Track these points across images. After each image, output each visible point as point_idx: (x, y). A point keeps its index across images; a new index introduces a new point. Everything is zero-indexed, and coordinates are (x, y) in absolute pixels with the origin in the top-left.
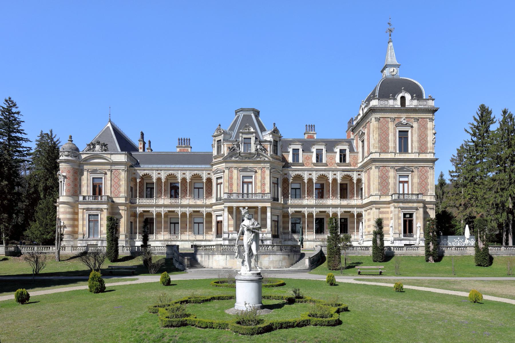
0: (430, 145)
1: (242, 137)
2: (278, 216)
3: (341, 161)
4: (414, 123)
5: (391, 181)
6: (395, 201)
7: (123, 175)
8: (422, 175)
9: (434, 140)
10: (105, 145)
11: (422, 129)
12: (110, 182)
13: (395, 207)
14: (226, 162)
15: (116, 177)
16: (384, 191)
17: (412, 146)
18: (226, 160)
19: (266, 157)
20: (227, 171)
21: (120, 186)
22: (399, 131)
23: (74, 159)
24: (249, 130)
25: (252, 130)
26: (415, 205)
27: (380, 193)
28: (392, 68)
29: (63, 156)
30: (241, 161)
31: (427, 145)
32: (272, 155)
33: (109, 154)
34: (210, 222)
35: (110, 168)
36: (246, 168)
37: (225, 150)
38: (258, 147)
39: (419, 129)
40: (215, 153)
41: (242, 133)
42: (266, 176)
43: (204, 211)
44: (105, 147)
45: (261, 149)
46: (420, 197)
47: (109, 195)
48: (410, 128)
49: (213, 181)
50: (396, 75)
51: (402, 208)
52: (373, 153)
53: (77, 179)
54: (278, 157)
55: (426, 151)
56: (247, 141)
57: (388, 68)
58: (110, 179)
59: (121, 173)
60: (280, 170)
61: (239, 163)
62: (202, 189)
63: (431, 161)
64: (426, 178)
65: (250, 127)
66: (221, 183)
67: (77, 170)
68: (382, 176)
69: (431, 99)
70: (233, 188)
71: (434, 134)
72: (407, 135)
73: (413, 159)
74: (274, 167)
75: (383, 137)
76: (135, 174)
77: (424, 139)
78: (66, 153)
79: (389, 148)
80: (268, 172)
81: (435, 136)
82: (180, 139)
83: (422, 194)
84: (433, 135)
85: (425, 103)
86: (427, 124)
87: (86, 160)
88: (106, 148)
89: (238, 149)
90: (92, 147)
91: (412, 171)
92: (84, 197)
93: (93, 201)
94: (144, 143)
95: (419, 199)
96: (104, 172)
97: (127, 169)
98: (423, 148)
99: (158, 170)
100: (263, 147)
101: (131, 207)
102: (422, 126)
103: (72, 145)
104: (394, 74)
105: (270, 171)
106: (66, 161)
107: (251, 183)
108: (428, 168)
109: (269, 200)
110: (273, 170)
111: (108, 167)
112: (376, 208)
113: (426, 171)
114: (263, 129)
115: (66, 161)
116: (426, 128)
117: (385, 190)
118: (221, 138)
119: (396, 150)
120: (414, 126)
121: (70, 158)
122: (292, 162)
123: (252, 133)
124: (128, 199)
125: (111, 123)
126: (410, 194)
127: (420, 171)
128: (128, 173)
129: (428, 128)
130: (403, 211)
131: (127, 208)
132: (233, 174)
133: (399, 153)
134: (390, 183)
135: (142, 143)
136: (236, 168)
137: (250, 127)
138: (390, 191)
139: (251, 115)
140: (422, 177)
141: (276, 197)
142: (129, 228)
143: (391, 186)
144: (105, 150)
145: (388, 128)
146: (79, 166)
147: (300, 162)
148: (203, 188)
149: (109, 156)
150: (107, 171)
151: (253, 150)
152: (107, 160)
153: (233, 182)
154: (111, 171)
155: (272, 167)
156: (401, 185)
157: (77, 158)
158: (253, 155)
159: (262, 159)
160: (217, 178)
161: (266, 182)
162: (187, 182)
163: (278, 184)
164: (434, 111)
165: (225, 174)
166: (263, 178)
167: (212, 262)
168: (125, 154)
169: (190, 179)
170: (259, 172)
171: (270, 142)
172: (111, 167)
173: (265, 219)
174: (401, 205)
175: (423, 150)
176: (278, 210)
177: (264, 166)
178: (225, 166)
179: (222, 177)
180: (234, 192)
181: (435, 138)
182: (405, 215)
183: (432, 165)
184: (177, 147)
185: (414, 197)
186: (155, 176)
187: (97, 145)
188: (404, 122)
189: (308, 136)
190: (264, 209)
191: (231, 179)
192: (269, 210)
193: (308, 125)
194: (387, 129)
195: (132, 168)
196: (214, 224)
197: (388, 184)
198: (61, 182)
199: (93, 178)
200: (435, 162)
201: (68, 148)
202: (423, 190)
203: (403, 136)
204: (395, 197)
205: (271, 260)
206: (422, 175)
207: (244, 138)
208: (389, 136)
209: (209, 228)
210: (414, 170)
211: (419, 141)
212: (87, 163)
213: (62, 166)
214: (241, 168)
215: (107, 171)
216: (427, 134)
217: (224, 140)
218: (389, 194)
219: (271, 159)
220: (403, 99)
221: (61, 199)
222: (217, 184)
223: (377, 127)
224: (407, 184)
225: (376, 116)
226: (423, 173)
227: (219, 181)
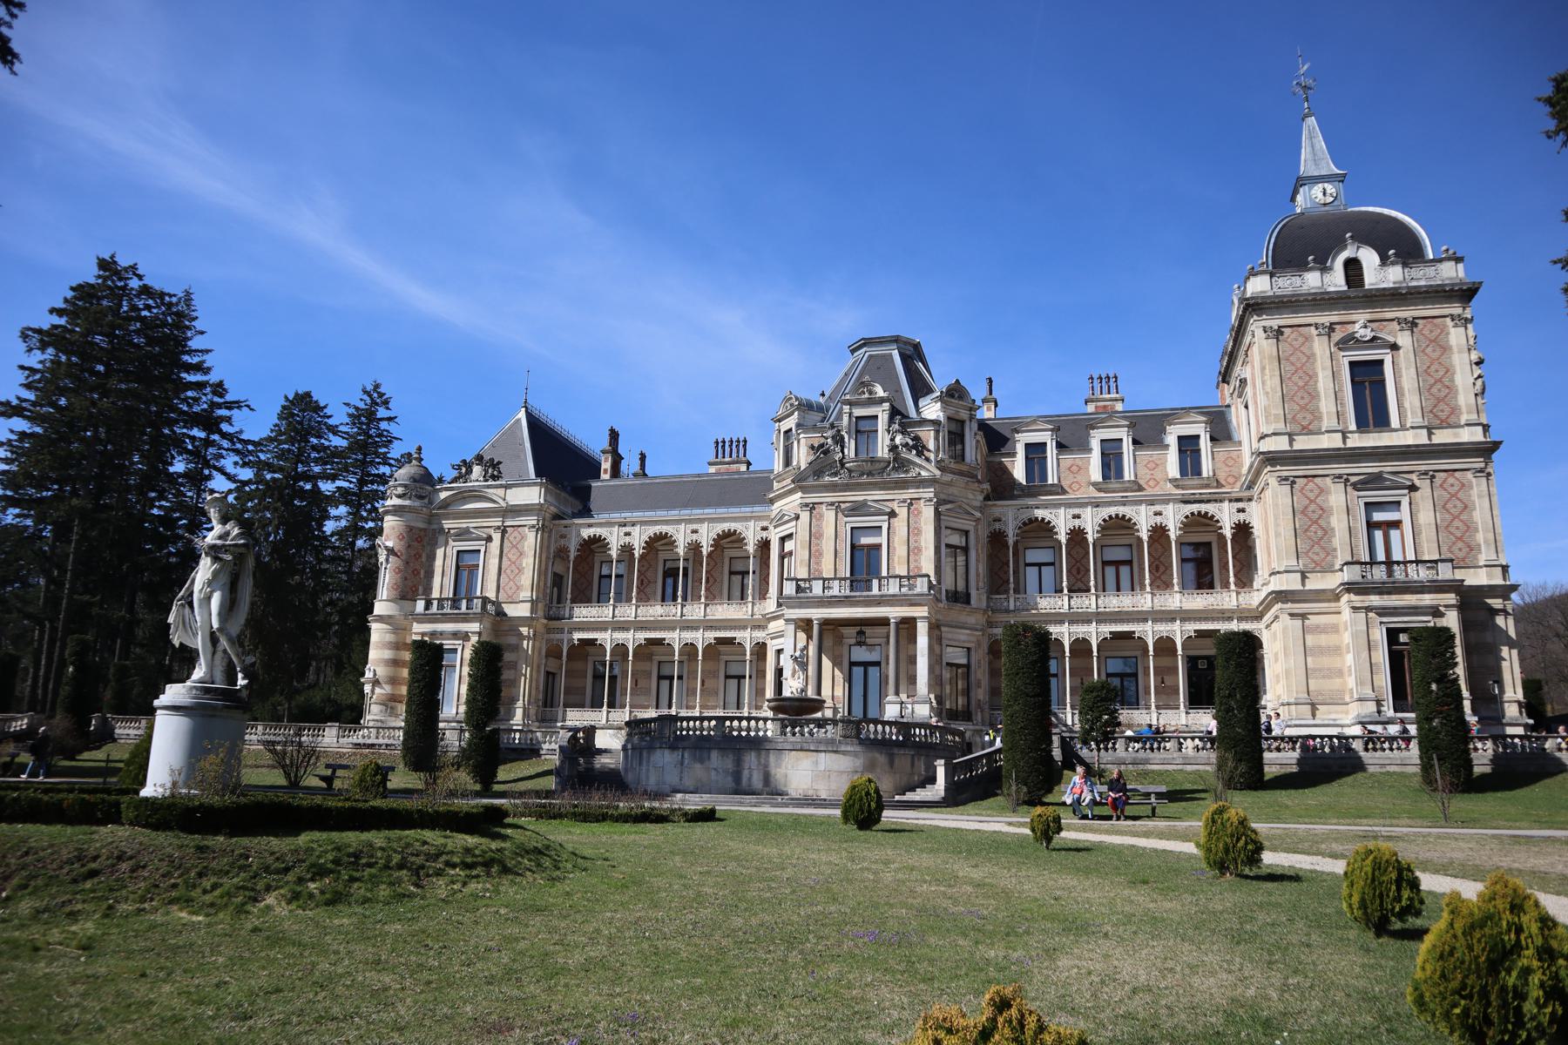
0: (1465, 398)
1: (850, 414)
2: (969, 649)
4: (1399, 333)
5: (1338, 522)
6: (1351, 587)
7: (530, 541)
8: (1449, 500)
9: (1479, 382)
10: (494, 465)
12: (497, 561)
13: (1354, 608)
14: (804, 490)
15: (514, 546)
16: (1316, 558)
17: (1399, 406)
18: (801, 482)
20: (805, 516)
21: (520, 570)
22: (1352, 364)
23: (417, 503)
24: (871, 393)
25: (880, 392)
26: (1427, 599)
27: (1304, 565)
28: (1320, 185)
30: (847, 485)
31: (1456, 400)
32: (942, 460)
33: (501, 486)
35: (500, 524)
36: (864, 504)
37: (802, 457)
38: (899, 439)
40: (778, 466)
41: (851, 404)
42: (922, 524)
43: (746, 637)
44: (494, 468)
46: (1445, 573)
47: (491, 595)
48: (1388, 351)
50: (1335, 203)
51: (1383, 612)
52: (1267, 436)
53: (420, 556)
54: (964, 468)
55: (1452, 420)
56: (864, 426)
57: (1306, 187)
58: (498, 552)
59: (526, 535)
60: (974, 508)
61: (840, 491)
63: (1477, 450)
64: (1466, 507)
65: (873, 386)
66: (790, 553)
67: (422, 533)
68: (1306, 508)
69: (1449, 259)
70: (823, 566)
71: (1477, 364)
72: (1382, 373)
73: (1409, 446)
74: (951, 498)
75: (1296, 384)
76: (563, 536)
78: (400, 490)
79: (1320, 419)
80: (928, 513)
81: (1479, 372)
83: (1451, 561)
84: (1474, 366)
85: (1430, 271)
86: (1448, 334)
87: (446, 504)
88: (495, 473)
89: (838, 449)
90: (464, 470)
91: (1413, 488)
92: (428, 605)
93: (449, 611)
95: (1440, 578)
96: (485, 536)
97: (543, 525)
98: (1442, 411)
99: (625, 525)
101: (549, 630)
102: (1431, 341)
103: (416, 468)
104: (1328, 201)
105: (936, 510)
106: (397, 510)
107: (878, 547)
108: (1469, 475)
109: (922, 595)
110: (949, 506)
111: (497, 522)
112: (1291, 615)
113: (1463, 485)
114: (920, 388)
115: (397, 510)
116: (1446, 349)
117: (1317, 554)
118: (790, 423)
120: (1400, 343)
121: (407, 503)
123: (882, 401)
124: (540, 605)
125: (526, 411)
126: (1411, 562)
127: (1441, 486)
128: (546, 535)
129: (1450, 348)
130: (1385, 619)
131: (535, 632)
132: (824, 523)
134: (1333, 529)
136: (832, 504)
137: (873, 386)
138: (1336, 557)
139: (891, 355)
140: (1449, 506)
141: (959, 589)
142: (537, 688)
143: (1339, 540)
144: (494, 478)
145: (1313, 355)
146: (430, 523)
149: (501, 492)
150: (491, 531)
151: (882, 451)
152: (494, 502)
153: (824, 548)
154: (504, 532)
155: (943, 496)
156: (1378, 535)
157: (426, 501)
158: (883, 465)
159: (912, 474)
160: (783, 540)
161: (923, 544)
163: (966, 550)
164: (1466, 294)
165: (799, 522)
167: (648, 770)
168: (541, 485)
170: (902, 512)
171: (935, 423)
172: (503, 522)
173: (913, 660)
174: (1375, 600)
175: (1439, 413)
176: (968, 631)
177: (916, 496)
178: (799, 501)
179: (792, 534)
181: (1479, 377)
182: (1392, 634)
183: (1482, 465)
185: (1423, 574)
186: (615, 539)
190: (908, 624)
191: (817, 538)
192: (922, 629)
194: (1309, 358)
195: (557, 522)
197: (1327, 532)
198: (382, 564)
199: (458, 552)
200: (1494, 456)
201: (406, 478)
202: (1460, 549)
203: (1367, 379)
204: (1349, 574)
205: (822, 768)
206: (1449, 500)
207: (857, 418)
208: (1316, 382)
210: (1417, 483)
212: (448, 514)
213: (390, 522)
214: (848, 505)
215: (491, 531)
216: (1452, 365)
217: (798, 425)
218: (1333, 565)
219: (938, 473)
221: (380, 608)
222: (782, 557)
223: (1275, 353)
224: (1398, 532)
226: (1453, 490)
227: (789, 546)
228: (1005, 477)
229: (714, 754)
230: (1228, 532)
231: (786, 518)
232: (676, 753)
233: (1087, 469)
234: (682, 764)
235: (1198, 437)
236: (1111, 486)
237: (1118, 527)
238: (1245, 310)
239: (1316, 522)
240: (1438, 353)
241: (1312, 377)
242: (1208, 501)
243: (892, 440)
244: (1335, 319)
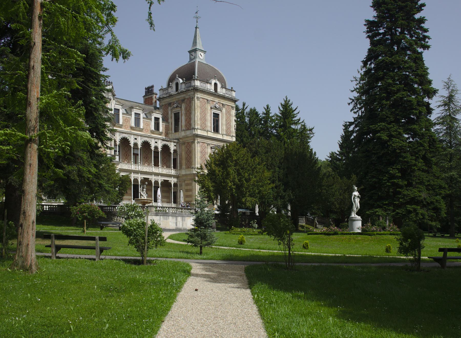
11: (227, 114)
39: (226, 114)
55: (230, 134)
77: (228, 123)
85: (229, 93)
116: (230, 115)
119: (211, 129)
188: (217, 106)
211: (226, 125)
220: (216, 85)
225: (198, 96)
229: (170, 218)
230: (172, 152)
232: (157, 217)
233: (130, 121)
234: (160, 220)
235: (159, 118)
236: (137, 129)
237: (146, 145)
238: (193, 89)
239: (204, 156)
242: (168, 141)
244: (212, 99)
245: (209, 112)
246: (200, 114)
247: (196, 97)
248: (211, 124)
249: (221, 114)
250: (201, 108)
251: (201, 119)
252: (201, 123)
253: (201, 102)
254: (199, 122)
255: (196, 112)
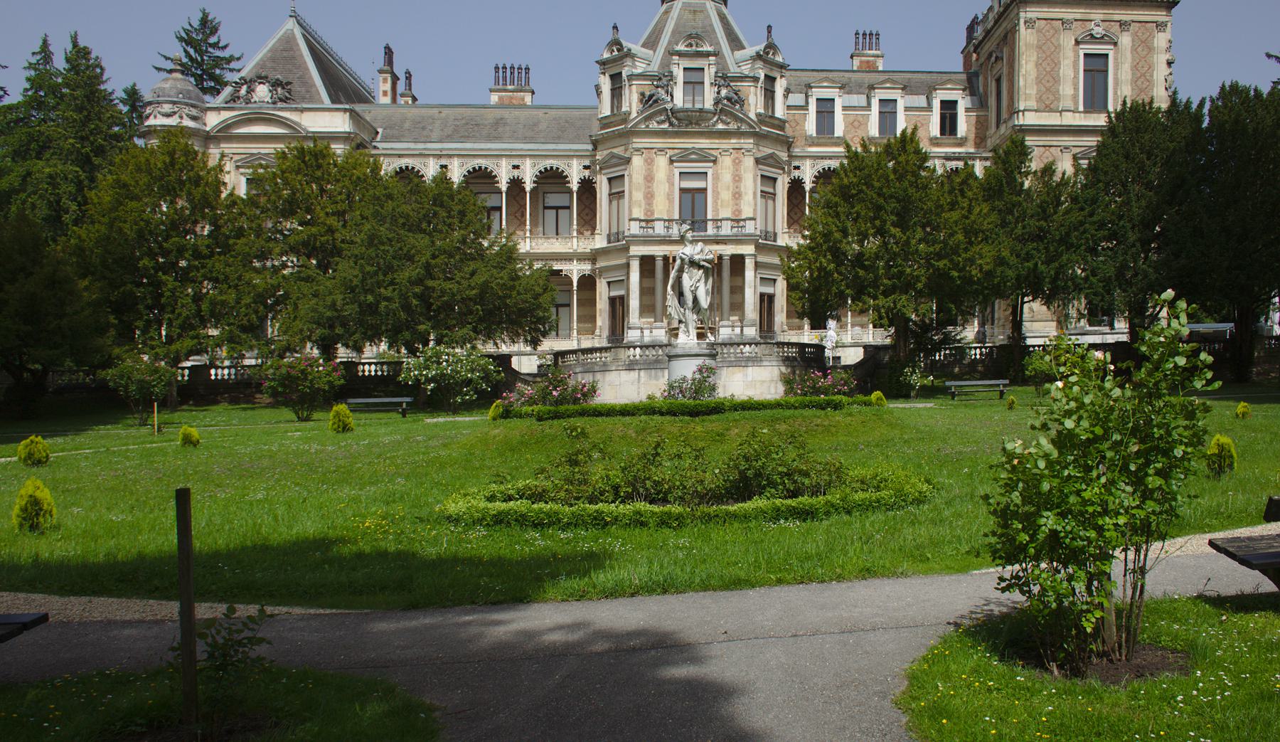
3: (943, 132)
19: (742, 120)
29: (155, 117)
33: (296, 110)
34: (588, 302)
39: (1134, 49)
45: (729, 99)
49: (597, 186)
62: (567, 211)
75: (1045, 69)
77: (1144, 75)
79: (1058, 99)
80: (749, 162)
82: (500, 66)
89: (669, 99)
94: (395, 79)
99: (440, 156)
100: (736, 94)
102: (1142, 42)
107: (705, 190)
116: (1150, 49)
119: (1076, 103)
122: (815, 135)
123: (708, 55)
133: (1085, 112)
135: (389, 76)
136: (661, 150)
145: (1058, 47)
147: (836, 135)
148: (569, 208)
162: (524, 189)
166: (737, 179)
169: (534, 182)
177: (737, 146)
180: (656, 216)
184: (491, 91)
187: (260, 83)
188: (1098, 31)
189: (861, 62)
193: (861, 33)
196: (602, 305)
209: (588, 318)
225: (1029, 15)
228: (798, 128)
231: (614, 161)
240: (1145, 53)
241: (1057, 64)
243: (718, 93)
244: (1078, 16)
245: (1070, 54)
246: (1037, 65)
247: (1022, 21)
248: (1076, 89)
249: (1116, 53)
250: (1039, 47)
251: (1039, 81)
252: (1039, 91)
253: (1039, 31)
254: (1032, 91)
255: (1024, 62)
